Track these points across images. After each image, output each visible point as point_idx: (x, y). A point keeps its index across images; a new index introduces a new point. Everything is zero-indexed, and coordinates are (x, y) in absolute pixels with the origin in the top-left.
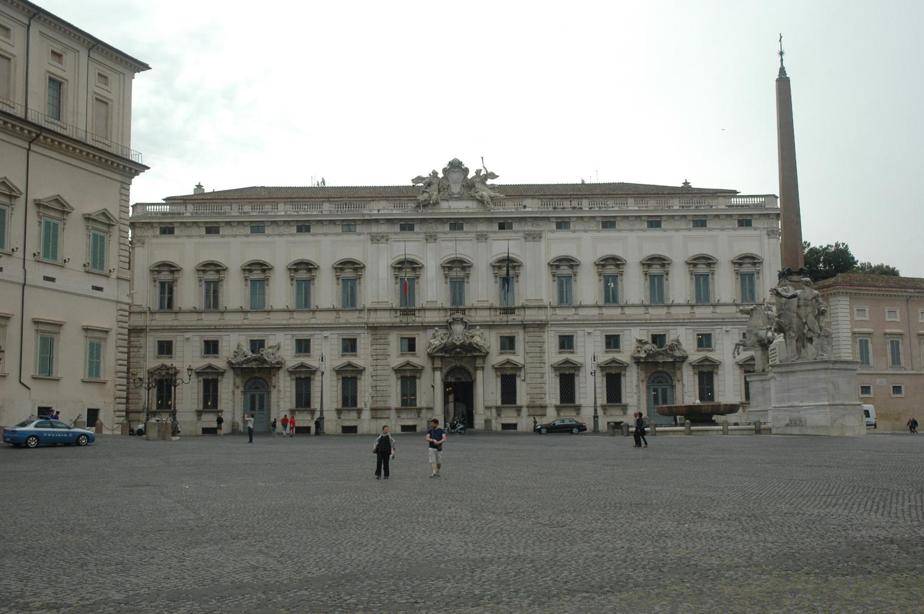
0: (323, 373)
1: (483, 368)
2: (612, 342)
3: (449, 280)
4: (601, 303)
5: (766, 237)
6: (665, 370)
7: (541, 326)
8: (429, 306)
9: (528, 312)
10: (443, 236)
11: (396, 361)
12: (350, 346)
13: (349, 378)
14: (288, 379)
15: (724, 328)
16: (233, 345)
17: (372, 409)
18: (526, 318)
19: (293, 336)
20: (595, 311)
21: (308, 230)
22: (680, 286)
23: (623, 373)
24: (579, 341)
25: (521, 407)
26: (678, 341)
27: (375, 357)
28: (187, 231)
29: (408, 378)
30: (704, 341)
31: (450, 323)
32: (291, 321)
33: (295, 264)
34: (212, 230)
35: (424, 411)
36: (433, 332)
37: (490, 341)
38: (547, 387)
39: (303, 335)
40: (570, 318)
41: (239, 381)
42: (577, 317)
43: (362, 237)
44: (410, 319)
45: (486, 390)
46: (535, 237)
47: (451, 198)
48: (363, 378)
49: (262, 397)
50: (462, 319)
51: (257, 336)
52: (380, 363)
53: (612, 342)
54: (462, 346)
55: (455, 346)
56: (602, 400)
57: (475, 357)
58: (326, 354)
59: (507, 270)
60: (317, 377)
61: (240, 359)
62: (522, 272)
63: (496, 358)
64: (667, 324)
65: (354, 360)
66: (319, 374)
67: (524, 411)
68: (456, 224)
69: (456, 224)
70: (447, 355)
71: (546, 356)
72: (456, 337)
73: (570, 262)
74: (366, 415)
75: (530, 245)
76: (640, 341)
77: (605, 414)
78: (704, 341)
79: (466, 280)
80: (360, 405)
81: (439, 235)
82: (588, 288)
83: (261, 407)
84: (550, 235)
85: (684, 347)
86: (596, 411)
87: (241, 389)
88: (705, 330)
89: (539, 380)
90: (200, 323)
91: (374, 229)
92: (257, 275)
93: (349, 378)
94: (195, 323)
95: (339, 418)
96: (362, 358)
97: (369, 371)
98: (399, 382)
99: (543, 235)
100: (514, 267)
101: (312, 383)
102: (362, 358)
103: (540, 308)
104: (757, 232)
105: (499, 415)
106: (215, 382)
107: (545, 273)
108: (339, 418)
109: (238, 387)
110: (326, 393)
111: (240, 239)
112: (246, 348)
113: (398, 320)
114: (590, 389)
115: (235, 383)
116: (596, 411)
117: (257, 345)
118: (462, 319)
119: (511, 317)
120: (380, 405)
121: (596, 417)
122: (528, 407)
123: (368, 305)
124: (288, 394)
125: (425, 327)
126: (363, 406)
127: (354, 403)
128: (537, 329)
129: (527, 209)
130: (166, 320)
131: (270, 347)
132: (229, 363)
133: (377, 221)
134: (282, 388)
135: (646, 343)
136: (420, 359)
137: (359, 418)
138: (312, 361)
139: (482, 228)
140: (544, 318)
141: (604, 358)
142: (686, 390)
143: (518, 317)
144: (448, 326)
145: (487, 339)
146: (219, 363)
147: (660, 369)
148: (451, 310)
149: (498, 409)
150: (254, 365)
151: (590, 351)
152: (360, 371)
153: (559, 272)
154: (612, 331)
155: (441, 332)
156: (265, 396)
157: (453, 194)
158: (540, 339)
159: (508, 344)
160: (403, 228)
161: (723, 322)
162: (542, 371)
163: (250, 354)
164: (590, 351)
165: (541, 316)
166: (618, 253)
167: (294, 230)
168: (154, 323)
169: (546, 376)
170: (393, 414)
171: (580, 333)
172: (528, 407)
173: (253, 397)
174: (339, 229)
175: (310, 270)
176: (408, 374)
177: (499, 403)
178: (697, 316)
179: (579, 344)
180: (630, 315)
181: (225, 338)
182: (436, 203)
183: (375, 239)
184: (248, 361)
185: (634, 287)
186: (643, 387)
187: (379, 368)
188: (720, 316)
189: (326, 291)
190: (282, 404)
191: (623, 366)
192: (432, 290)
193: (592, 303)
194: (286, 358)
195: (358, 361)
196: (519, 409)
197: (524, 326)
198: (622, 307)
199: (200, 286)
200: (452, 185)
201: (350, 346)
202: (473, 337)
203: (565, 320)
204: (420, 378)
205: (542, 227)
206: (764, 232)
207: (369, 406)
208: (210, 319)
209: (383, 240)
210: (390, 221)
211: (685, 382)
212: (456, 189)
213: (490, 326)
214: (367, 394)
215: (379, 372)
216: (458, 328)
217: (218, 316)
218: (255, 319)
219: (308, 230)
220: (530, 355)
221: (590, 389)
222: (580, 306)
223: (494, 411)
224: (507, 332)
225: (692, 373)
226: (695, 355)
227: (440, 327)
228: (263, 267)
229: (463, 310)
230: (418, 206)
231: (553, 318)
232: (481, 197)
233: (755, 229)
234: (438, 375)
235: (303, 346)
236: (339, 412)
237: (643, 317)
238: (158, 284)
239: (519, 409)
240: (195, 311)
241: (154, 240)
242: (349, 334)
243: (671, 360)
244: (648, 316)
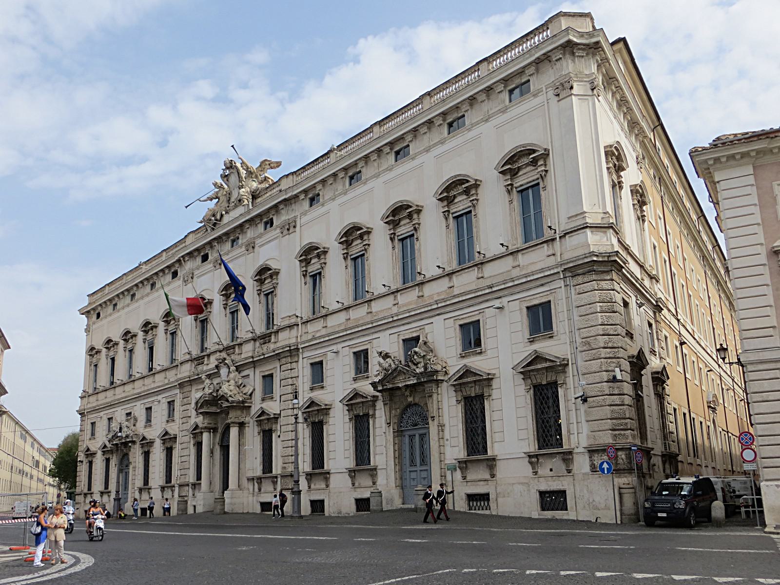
6: (417, 400)
7: (293, 352)
9: (282, 335)
23: (371, 413)
40: (318, 335)
64: (420, 316)
78: (472, 337)
88: (468, 314)
128: (289, 359)
158: (294, 374)
164: (340, 382)
171: (330, 355)
203: (314, 338)
213: (254, 364)
225: (453, 401)
243: (415, 381)
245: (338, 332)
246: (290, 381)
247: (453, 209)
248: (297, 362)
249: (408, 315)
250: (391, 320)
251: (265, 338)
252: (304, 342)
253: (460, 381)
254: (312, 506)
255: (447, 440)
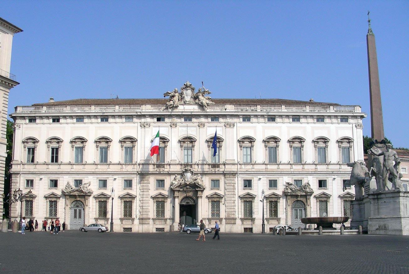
0: (113, 199)
1: (201, 197)
2: (273, 184)
3: (183, 148)
4: (267, 162)
5: (354, 128)
7: (234, 174)
8: (171, 163)
10: (180, 124)
11: (153, 191)
12: (129, 184)
13: (128, 202)
14: (95, 201)
15: (333, 177)
16: (65, 182)
17: (139, 219)
18: (226, 170)
19: (97, 178)
20: (264, 167)
21: (107, 120)
22: (310, 153)
24: (255, 183)
25: (222, 219)
26: (308, 183)
27: (142, 190)
28: (42, 121)
29: (160, 202)
30: (322, 184)
31: (184, 172)
32: (97, 170)
33: (100, 139)
34: (56, 120)
35: (168, 221)
36: (174, 176)
37: (206, 182)
38: (236, 208)
39: (103, 177)
40: (249, 170)
41: (69, 202)
42: (253, 170)
43: (136, 125)
44: (162, 169)
45: (204, 209)
46: (232, 125)
47: (185, 103)
48: (135, 201)
49: (80, 211)
50: (190, 170)
51: (78, 177)
52: (145, 194)
53: (273, 184)
54: (190, 185)
55: (186, 185)
56: (267, 215)
57: (197, 191)
58: (116, 188)
59: (215, 142)
60: (110, 201)
61: (70, 190)
62: (223, 144)
63: (208, 192)
65: (131, 192)
66: (111, 199)
67: (224, 221)
68: (188, 117)
69: (188, 117)
70: (181, 190)
71: (236, 191)
72: (186, 180)
73: (251, 140)
74: (136, 222)
75: (229, 130)
76: (288, 183)
77: (268, 223)
78: (322, 184)
79: (193, 148)
80: (134, 216)
81: (178, 124)
82: (260, 153)
83: (80, 217)
84: (239, 125)
85: (311, 187)
86: (263, 221)
87: (69, 206)
89: (233, 204)
90: (48, 170)
91: (143, 120)
92: (79, 145)
93: (128, 202)
94: (45, 170)
95: (122, 223)
96: (135, 190)
97: (138, 198)
98: (155, 204)
99: (235, 125)
100: (219, 142)
101: (107, 203)
102: (135, 190)
103: (233, 164)
104: (351, 125)
105: (210, 223)
106: (56, 202)
107: (236, 145)
108: (122, 223)
109: (67, 205)
110: (116, 209)
111: (70, 125)
112: (72, 184)
113: (155, 170)
114: (260, 209)
115: (66, 203)
116: (263, 221)
117: (78, 182)
118: (190, 170)
119: (217, 169)
120: (144, 216)
121: (263, 225)
122: (225, 219)
123: (138, 162)
124: (94, 210)
125: (169, 174)
126: (135, 217)
127: (131, 215)
128: (232, 176)
129: (227, 110)
130: (30, 168)
131: (85, 184)
132: (63, 192)
133: (144, 116)
134: (91, 206)
135: (291, 184)
136: (166, 192)
137: (133, 223)
138: (107, 192)
139: (203, 120)
140: (236, 170)
141: (268, 192)
142: (312, 210)
143: (222, 169)
144: (182, 174)
145: (204, 181)
146: (58, 192)
147: (299, 199)
148: (184, 165)
149: (209, 220)
150: (76, 193)
151: (260, 188)
152: (133, 197)
153: (244, 145)
154: (273, 178)
155: (179, 177)
156: (82, 211)
157: (186, 101)
158: (233, 182)
159: (215, 184)
160: (159, 120)
161: (332, 173)
162: (233, 199)
163: (74, 187)
164: (260, 188)
165: (234, 168)
166: (276, 135)
167: (99, 120)
168: (24, 170)
169: (236, 202)
170: (151, 221)
172: (225, 219)
173: (75, 211)
174: (124, 120)
175: (107, 142)
176: (160, 200)
177: (210, 217)
178: (319, 170)
179: (254, 185)
180: (283, 169)
181: (61, 179)
182: (177, 107)
183: (143, 126)
184: (73, 191)
185: (285, 153)
186: (289, 209)
187: (144, 196)
188: (331, 171)
189: (116, 153)
190: (90, 215)
191: (277, 197)
192: (174, 153)
193: (261, 162)
194: (93, 190)
195: (132, 192)
196: (221, 220)
197: (224, 174)
198: (278, 165)
199: (49, 150)
200: (186, 97)
201: (129, 184)
202: (196, 180)
204: (166, 202)
205: (235, 120)
206: (354, 125)
207: (138, 217)
208: (54, 168)
209: (148, 126)
210: (152, 116)
211: (312, 206)
212: (188, 98)
214: (137, 211)
215: (144, 199)
216: (189, 175)
217: (58, 166)
218: (77, 168)
219: (107, 120)
220: (228, 190)
221: (260, 209)
222: (255, 164)
223: (207, 221)
224: (215, 177)
226: (317, 191)
227: (178, 174)
228: (83, 140)
229: (191, 165)
230: (167, 108)
231: (241, 170)
232: (202, 103)
233: (349, 124)
234: (177, 201)
235: (104, 184)
236: (121, 219)
237: (289, 170)
238: (27, 150)
239: (221, 220)
240: (45, 164)
241: (25, 126)
242: (128, 177)
243: (305, 194)
244: (292, 170)
245: (261, 172)
246: (232, 185)
247: (318, 145)
248: (235, 178)
249: (298, 173)
250: (290, 173)
251: (215, 166)
252: (240, 172)
253: (320, 196)
254: (244, 230)
255: (312, 212)
